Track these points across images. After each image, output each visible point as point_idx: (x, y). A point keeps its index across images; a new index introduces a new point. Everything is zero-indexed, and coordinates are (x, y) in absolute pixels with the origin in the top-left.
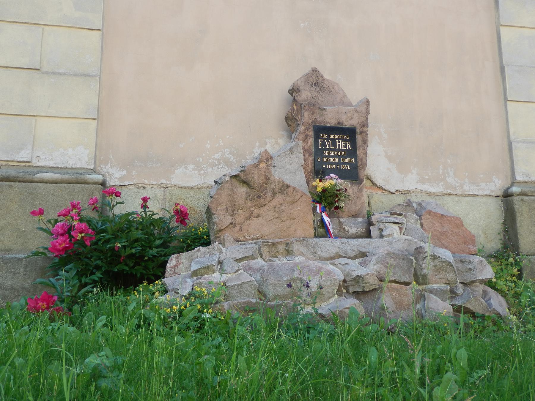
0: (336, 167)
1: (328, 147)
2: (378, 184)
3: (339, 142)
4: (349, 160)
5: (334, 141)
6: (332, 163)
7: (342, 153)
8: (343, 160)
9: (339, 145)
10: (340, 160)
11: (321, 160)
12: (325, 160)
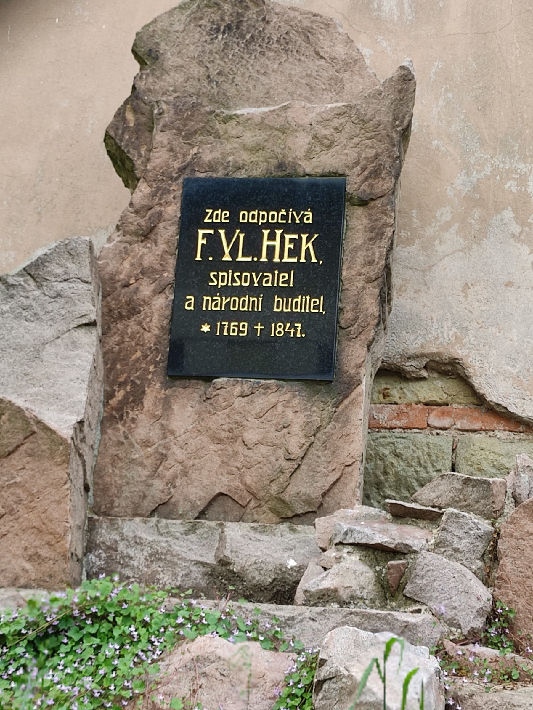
0: (252, 331)
1: (227, 258)
2: (492, 397)
3: (272, 237)
4: (308, 304)
5: (253, 233)
6: (238, 316)
7: (283, 279)
8: (281, 305)
9: (271, 250)
10: (268, 303)
11: (198, 303)
12: (214, 304)
